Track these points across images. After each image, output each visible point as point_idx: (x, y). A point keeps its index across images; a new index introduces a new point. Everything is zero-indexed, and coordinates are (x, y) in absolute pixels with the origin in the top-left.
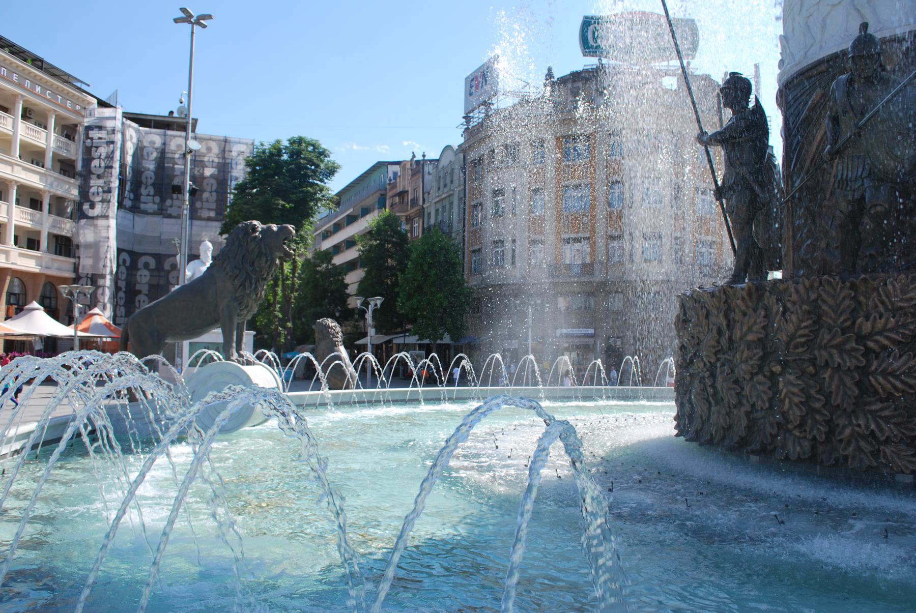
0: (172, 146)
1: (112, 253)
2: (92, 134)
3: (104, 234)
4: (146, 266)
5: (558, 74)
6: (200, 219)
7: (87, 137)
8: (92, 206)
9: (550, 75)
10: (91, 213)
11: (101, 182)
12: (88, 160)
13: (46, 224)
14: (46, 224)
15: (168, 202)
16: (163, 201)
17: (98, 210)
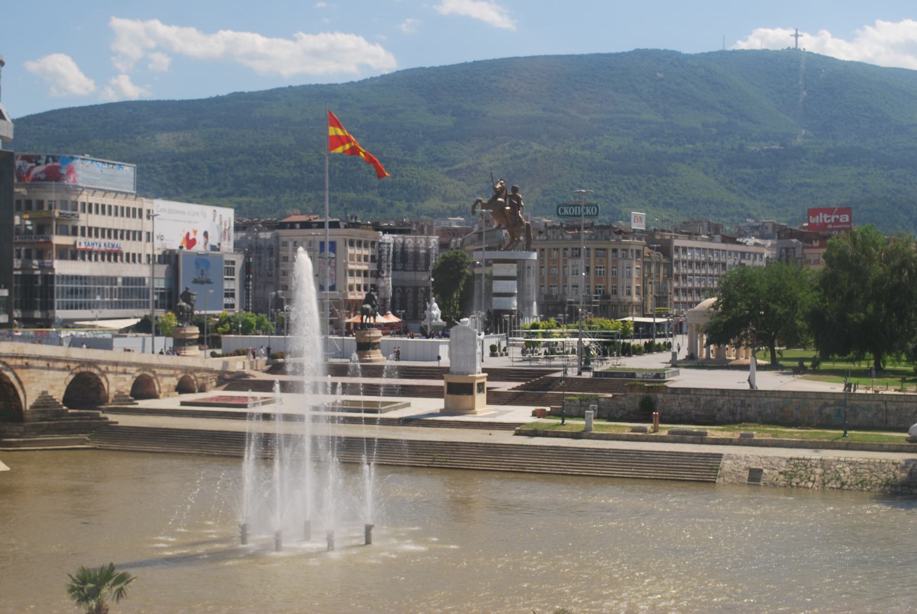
0: (407, 242)
5: (548, 225)
12: (380, 256)
13: (370, 281)
14: (370, 281)
17: (385, 274)
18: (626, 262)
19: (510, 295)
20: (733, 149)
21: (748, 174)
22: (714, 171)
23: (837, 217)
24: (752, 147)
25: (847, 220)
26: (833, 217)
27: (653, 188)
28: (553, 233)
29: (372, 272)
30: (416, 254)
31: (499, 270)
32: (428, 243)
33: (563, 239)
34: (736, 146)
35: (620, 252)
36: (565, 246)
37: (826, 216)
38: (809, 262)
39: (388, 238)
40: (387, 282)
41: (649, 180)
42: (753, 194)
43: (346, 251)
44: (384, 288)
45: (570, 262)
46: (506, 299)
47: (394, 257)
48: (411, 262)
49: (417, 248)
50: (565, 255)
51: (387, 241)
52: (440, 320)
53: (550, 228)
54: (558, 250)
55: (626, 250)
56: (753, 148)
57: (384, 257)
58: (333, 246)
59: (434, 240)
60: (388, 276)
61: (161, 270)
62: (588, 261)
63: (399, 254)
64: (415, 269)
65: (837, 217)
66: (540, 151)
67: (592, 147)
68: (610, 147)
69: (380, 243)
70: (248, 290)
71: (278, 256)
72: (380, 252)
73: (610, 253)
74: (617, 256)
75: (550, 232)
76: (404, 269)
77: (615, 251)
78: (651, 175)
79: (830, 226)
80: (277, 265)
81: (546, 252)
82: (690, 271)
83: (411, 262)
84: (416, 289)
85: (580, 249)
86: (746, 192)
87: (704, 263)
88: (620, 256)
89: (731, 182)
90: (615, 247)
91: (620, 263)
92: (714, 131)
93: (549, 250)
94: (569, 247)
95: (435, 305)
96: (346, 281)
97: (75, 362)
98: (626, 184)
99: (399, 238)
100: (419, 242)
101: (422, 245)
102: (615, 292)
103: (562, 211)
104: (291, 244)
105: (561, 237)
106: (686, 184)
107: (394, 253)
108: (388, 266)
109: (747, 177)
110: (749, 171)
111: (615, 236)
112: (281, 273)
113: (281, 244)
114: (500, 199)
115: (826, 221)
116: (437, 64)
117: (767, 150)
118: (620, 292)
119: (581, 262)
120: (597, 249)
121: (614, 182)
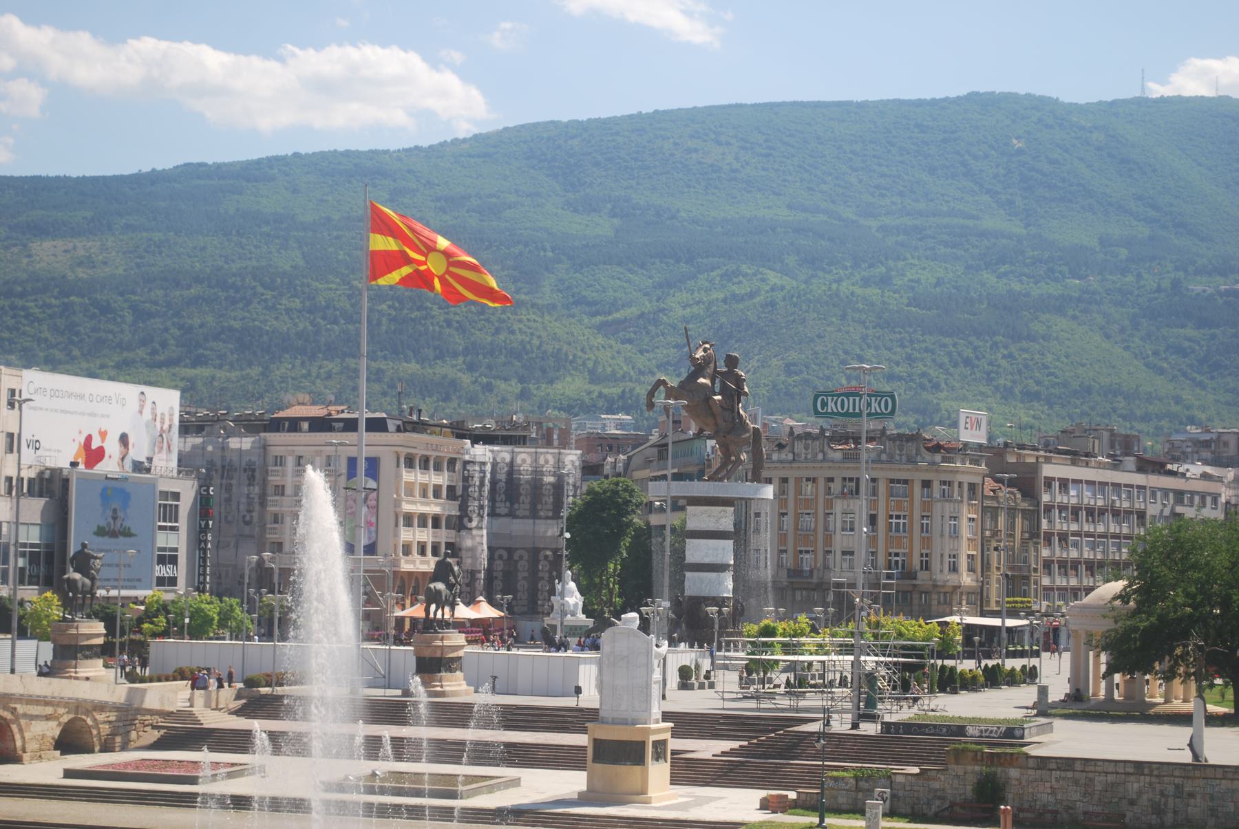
0: (519, 460)
1: (485, 555)
2: (468, 467)
3: (478, 539)
4: (500, 557)
5: (797, 432)
6: (540, 518)
7: (465, 468)
8: (470, 520)
10: (469, 525)
11: (476, 503)
12: (465, 488)
13: (444, 535)
14: (444, 535)
15: (516, 506)
16: (512, 504)
17: (474, 524)
18: (948, 508)
19: (719, 568)
20: (1159, 290)
21: (1189, 339)
22: (1122, 330)
24: (1198, 286)
27: (1004, 363)
28: (806, 448)
29: (449, 518)
30: (536, 485)
31: (698, 518)
32: (559, 463)
33: (824, 460)
34: (1166, 284)
35: (936, 486)
36: (830, 474)
39: (481, 452)
40: (478, 539)
41: (995, 346)
42: (1199, 378)
43: (398, 476)
44: (472, 550)
45: (839, 506)
46: (714, 575)
47: (493, 490)
48: (525, 500)
49: (537, 472)
50: (828, 491)
51: (479, 459)
52: (583, 617)
53: (799, 437)
54: (815, 480)
55: (949, 483)
56: (1199, 288)
57: (473, 491)
58: (373, 466)
59: (572, 458)
61: (34, 508)
62: (874, 504)
63: (502, 485)
64: (534, 515)
66: (783, 288)
67: (884, 281)
68: (918, 281)
69: (466, 463)
70: (205, 550)
71: (265, 482)
72: (466, 479)
73: (917, 489)
74: (930, 496)
75: (799, 447)
76: (512, 514)
77: (926, 484)
78: (999, 338)
80: (263, 504)
81: (791, 483)
82: (1074, 527)
83: (525, 500)
84: (535, 552)
85: (858, 479)
86: (1184, 374)
87: (1102, 512)
88: (936, 495)
89: (1156, 353)
90: (927, 477)
91: (937, 507)
92: (1124, 253)
93: (798, 480)
94: (837, 474)
95: (572, 585)
96: (396, 535)
97: (66, 705)
98: (949, 354)
99: (504, 453)
100: (542, 461)
101: (549, 468)
102: (926, 566)
103: (824, 404)
104: (290, 462)
105: (820, 456)
106: (1067, 357)
107: (494, 482)
108: (481, 507)
109: (1187, 344)
110: (1190, 332)
111: (928, 456)
112: (269, 518)
113: (270, 460)
114: (701, 380)
116: (702, 102)
117: (1228, 293)
118: (936, 565)
119: (860, 507)
120: (892, 481)
121: (926, 350)
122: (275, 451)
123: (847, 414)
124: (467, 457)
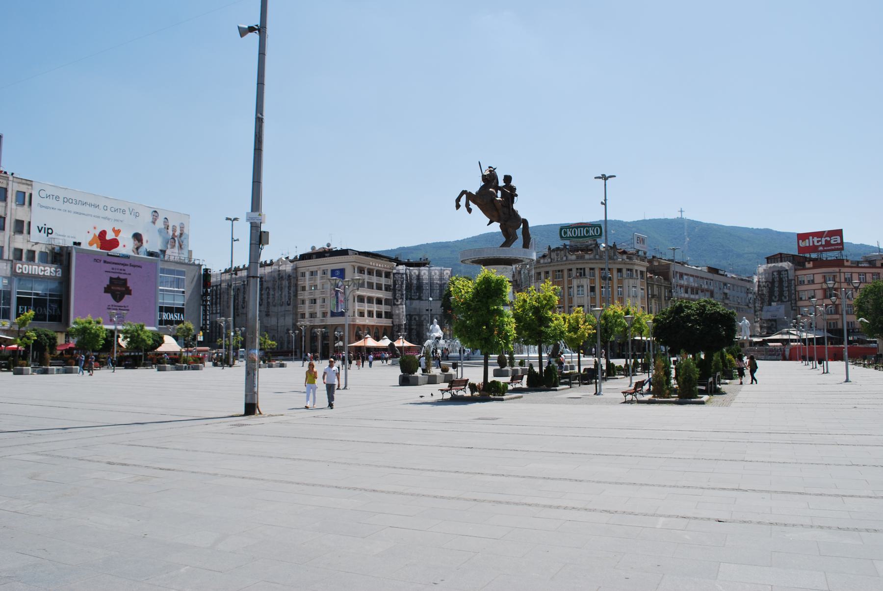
0: (422, 273)
5: (553, 247)
9: (549, 248)
18: (631, 281)
23: (828, 239)
25: (839, 241)
26: (823, 240)
29: (386, 300)
30: (431, 284)
35: (624, 271)
36: (570, 267)
37: (816, 239)
38: (802, 283)
40: (402, 310)
44: (399, 315)
45: (575, 283)
49: (431, 278)
50: (569, 276)
53: (554, 250)
54: (562, 271)
55: (631, 270)
60: (401, 304)
62: (593, 281)
65: (828, 239)
69: (394, 274)
70: (205, 306)
71: (296, 285)
74: (622, 276)
75: (554, 255)
77: (620, 270)
79: (821, 248)
80: (296, 295)
81: (551, 273)
82: (686, 296)
87: (697, 289)
88: (625, 276)
90: (619, 266)
91: (626, 282)
94: (574, 267)
95: (438, 326)
103: (565, 233)
104: (307, 274)
105: (565, 258)
111: (619, 256)
112: (299, 302)
113: (299, 274)
115: (816, 244)
119: (586, 282)
122: (301, 270)
123: (577, 237)
124: (395, 271)
